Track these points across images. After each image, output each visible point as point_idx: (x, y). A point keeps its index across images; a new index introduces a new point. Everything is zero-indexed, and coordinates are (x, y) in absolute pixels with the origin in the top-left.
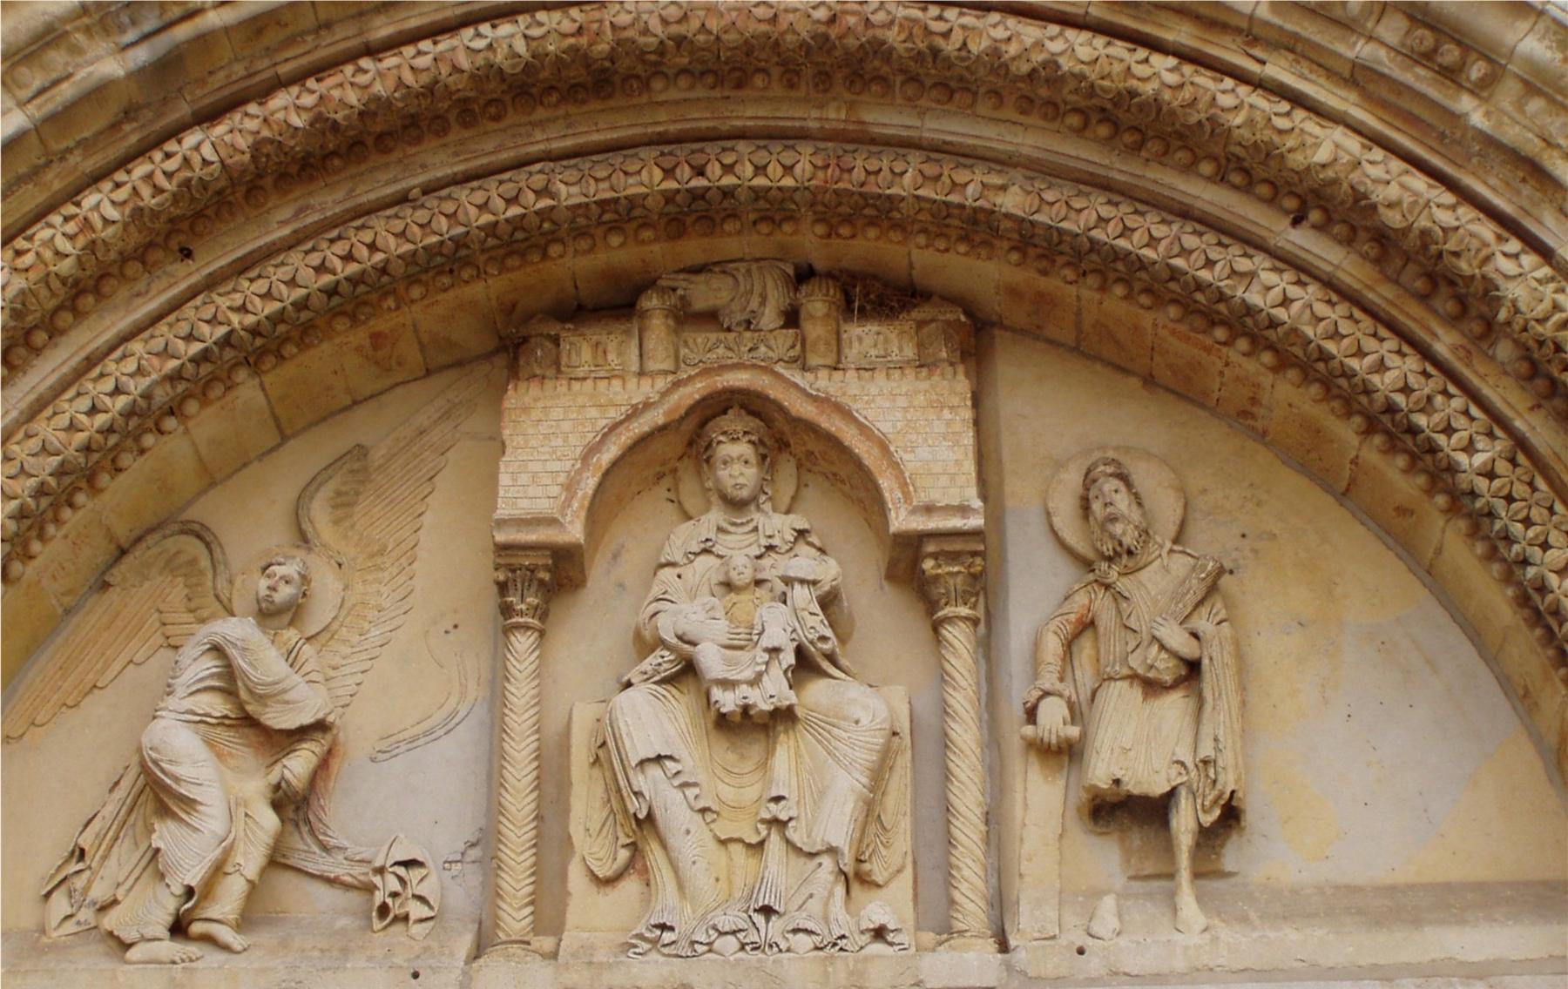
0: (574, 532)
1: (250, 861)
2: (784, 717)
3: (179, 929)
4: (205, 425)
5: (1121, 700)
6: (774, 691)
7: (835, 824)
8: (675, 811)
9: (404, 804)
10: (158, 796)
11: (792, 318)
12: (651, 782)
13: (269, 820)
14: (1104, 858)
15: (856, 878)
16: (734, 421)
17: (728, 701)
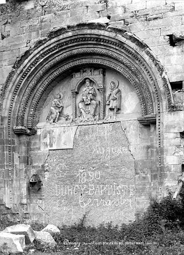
0: (76, 91)
1: (57, 117)
2: (90, 104)
3: (54, 122)
4: (52, 85)
5: (112, 101)
6: (89, 102)
7: (92, 112)
8: (83, 112)
9: (69, 111)
10: (52, 113)
11: (91, 71)
12: (81, 110)
13: (59, 114)
14: (112, 113)
15: (94, 116)
16: (87, 80)
17: (86, 103)
